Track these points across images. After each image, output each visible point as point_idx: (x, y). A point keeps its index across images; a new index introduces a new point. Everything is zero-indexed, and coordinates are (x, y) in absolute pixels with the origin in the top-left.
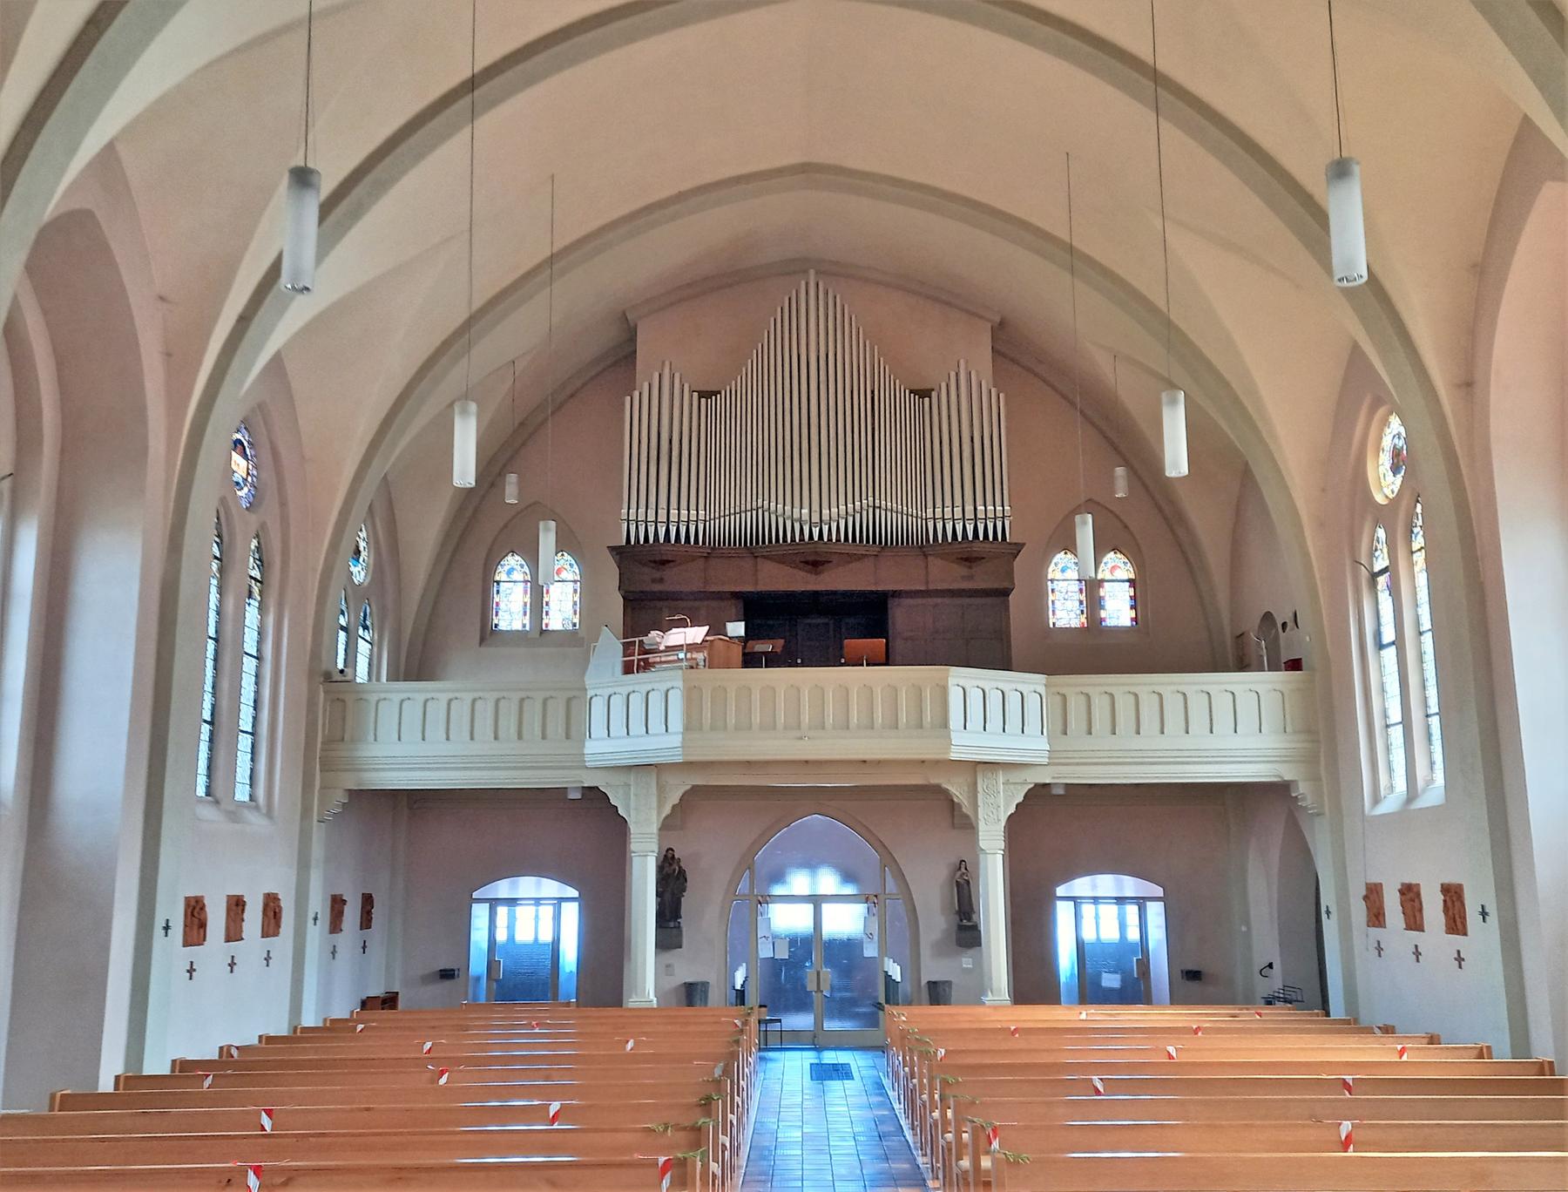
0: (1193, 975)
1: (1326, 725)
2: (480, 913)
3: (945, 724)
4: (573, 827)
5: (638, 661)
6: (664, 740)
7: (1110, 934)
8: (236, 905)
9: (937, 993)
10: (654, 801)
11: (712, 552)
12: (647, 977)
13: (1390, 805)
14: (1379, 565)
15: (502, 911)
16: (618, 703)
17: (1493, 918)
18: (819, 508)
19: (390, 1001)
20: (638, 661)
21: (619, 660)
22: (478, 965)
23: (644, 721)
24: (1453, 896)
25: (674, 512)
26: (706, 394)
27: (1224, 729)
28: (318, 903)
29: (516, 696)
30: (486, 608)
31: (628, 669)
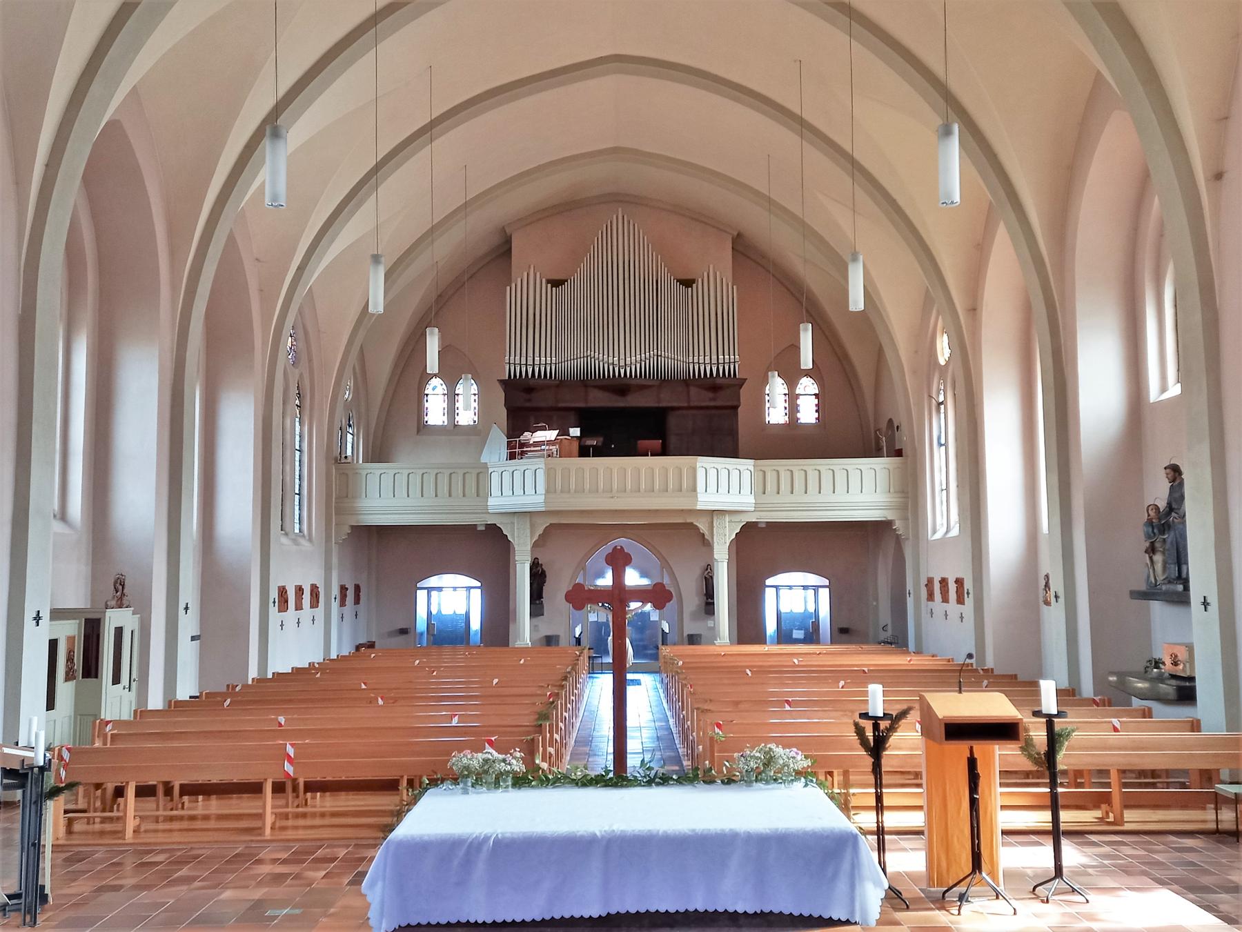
0: (844, 631)
1: (910, 490)
2: (421, 596)
3: (694, 489)
4: (481, 549)
5: (516, 451)
6: (534, 499)
7: (798, 609)
8: (300, 590)
9: (693, 640)
10: (528, 531)
11: (561, 384)
12: (525, 630)
13: (938, 536)
14: (941, 399)
15: (434, 593)
16: (507, 476)
17: (1062, 600)
18: (624, 357)
19: (371, 645)
20: (516, 451)
21: (504, 452)
22: (421, 624)
23: (523, 485)
24: (959, 582)
25: (537, 359)
26: (556, 283)
27: (853, 490)
28: (335, 591)
29: (447, 472)
30: (420, 411)
31: (512, 456)
